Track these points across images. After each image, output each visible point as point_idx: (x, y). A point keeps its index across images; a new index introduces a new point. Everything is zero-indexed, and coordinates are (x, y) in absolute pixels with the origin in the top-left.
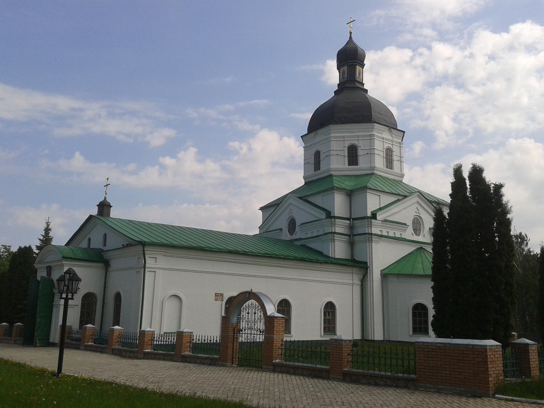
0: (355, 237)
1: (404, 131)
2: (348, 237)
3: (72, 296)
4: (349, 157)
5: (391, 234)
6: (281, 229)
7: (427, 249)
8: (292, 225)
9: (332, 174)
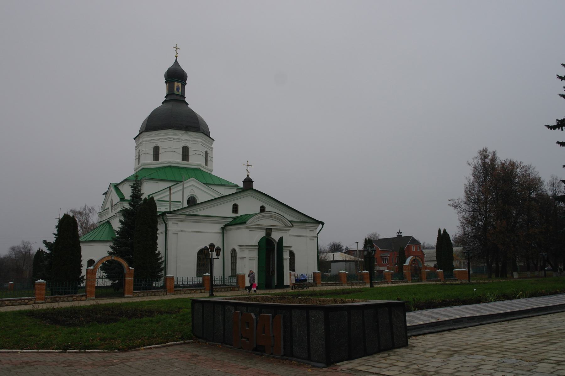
4: (183, 155)
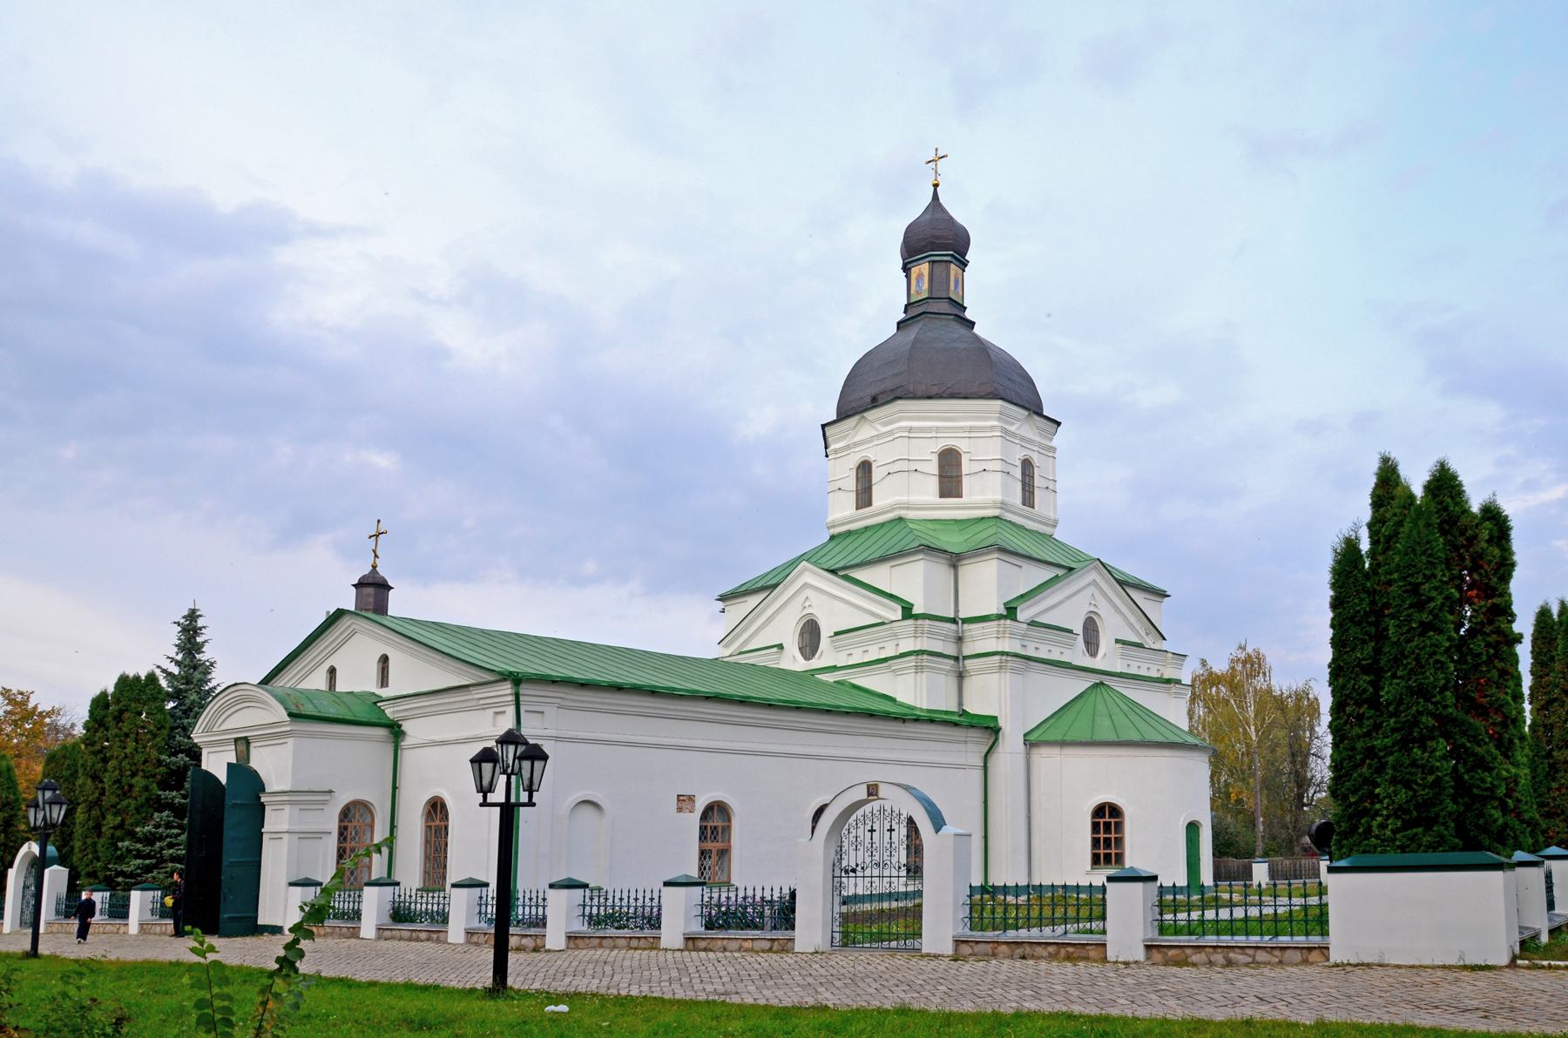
0: (967, 662)
1: (1059, 421)
2: (952, 662)
3: (530, 797)
5: (1043, 654)
6: (781, 647)
7: (1114, 687)
8: (810, 635)
9: (903, 516)
